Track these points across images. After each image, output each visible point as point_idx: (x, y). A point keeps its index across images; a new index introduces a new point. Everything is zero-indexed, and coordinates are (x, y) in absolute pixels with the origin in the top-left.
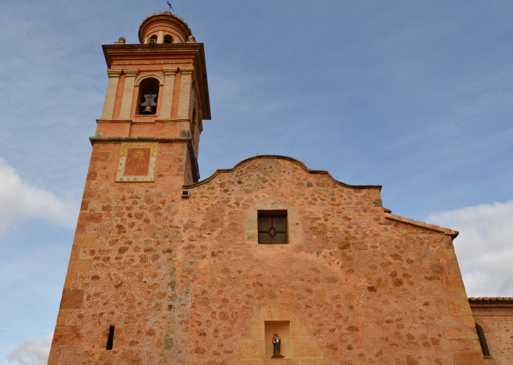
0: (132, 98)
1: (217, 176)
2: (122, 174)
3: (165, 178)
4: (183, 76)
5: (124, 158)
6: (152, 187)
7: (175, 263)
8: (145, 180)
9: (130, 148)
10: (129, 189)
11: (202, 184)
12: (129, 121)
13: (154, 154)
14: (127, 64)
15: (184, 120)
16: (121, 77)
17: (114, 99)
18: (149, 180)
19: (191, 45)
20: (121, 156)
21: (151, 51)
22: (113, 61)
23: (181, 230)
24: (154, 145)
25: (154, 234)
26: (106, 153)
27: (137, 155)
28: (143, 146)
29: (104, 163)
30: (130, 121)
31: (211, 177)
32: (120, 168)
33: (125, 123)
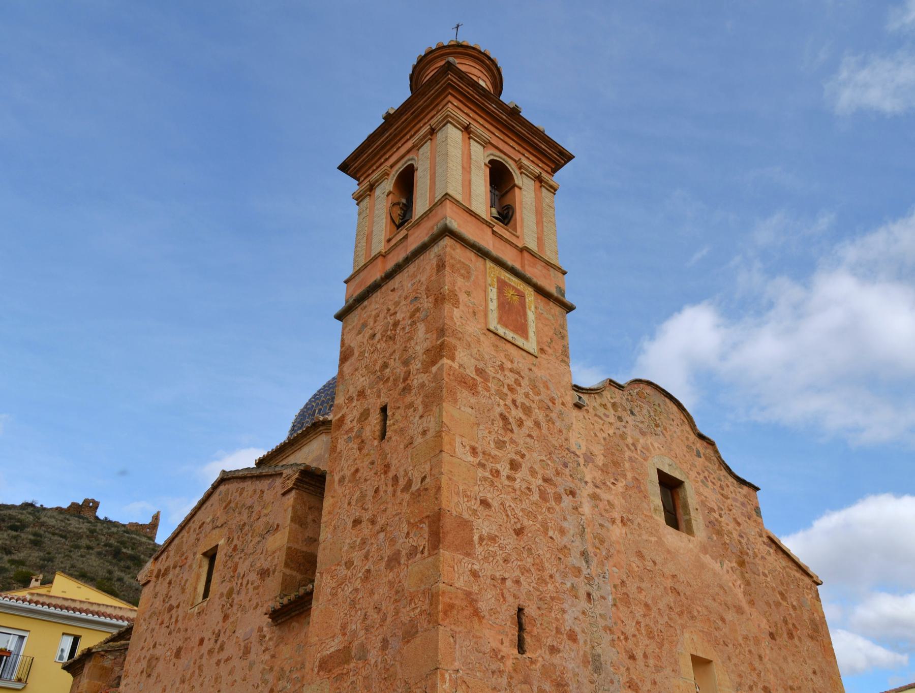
5: (495, 290)
7: (583, 517)
11: (593, 394)
15: (560, 269)
19: (560, 149)
21: (507, 119)
23: (581, 461)
25: (550, 454)
33: (485, 226)
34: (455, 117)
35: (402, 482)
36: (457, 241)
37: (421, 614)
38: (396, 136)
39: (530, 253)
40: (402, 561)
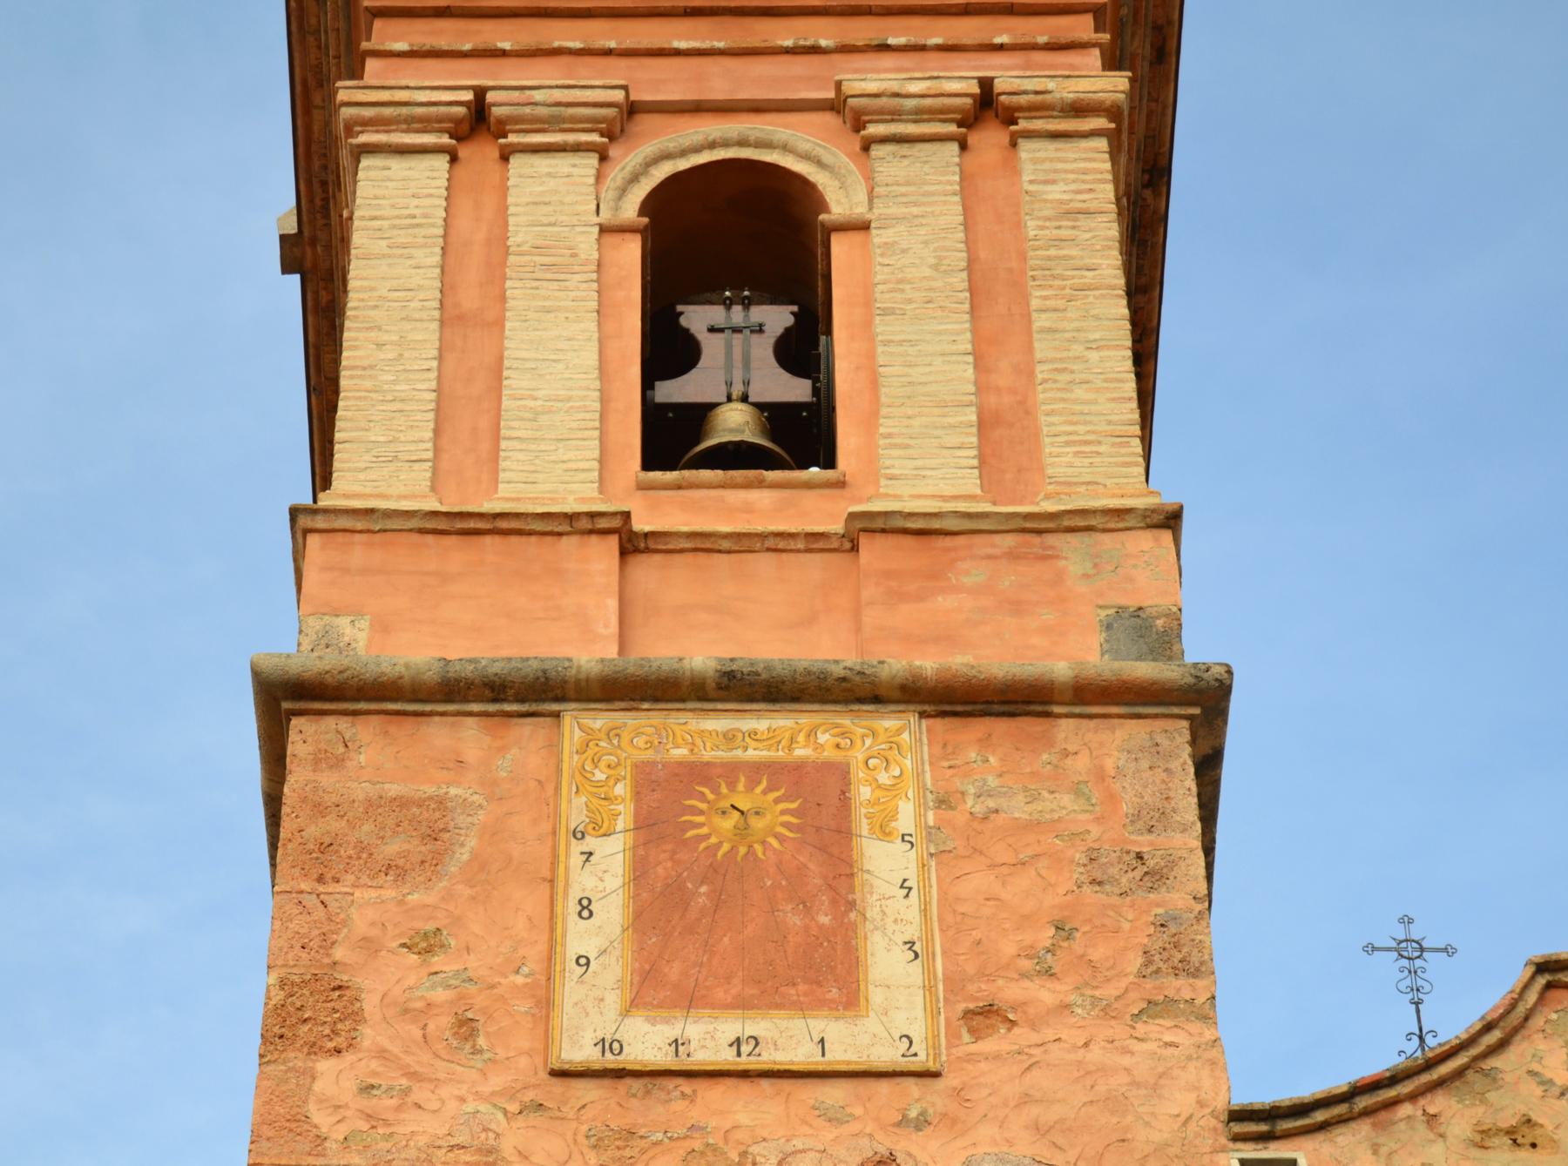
0: (593, 326)
1: (1538, 1021)
2: (613, 1001)
3: (1035, 1038)
4: (1027, 149)
6: (921, 1123)
8: (841, 1055)
9: (649, 755)
10: (697, 1145)
11: (1413, 1097)
12: (603, 524)
13: (893, 816)
14: (507, 46)
16: (464, 152)
17: (428, 334)
18: (887, 1055)
20: (579, 835)
22: (378, 24)
24: (874, 734)
26: (420, 804)
27: (729, 823)
28: (772, 738)
29: (414, 898)
30: (616, 523)
31: (1488, 1027)
32: (580, 938)
34: (388, 112)
36: (355, 713)
39: (906, 532)
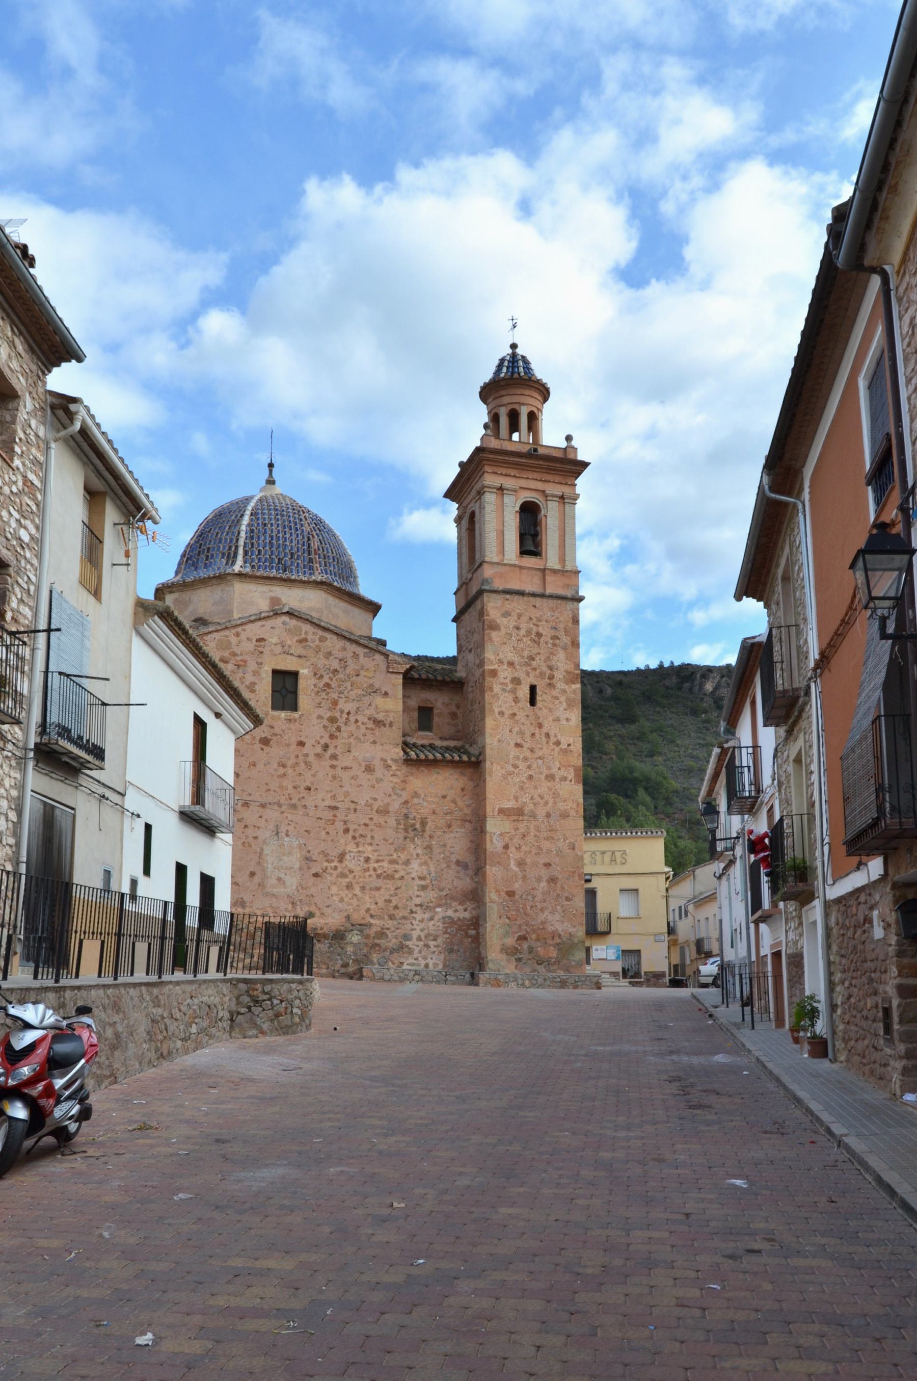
35: (553, 740)
37: (571, 808)
38: (527, 466)
40: (556, 780)
